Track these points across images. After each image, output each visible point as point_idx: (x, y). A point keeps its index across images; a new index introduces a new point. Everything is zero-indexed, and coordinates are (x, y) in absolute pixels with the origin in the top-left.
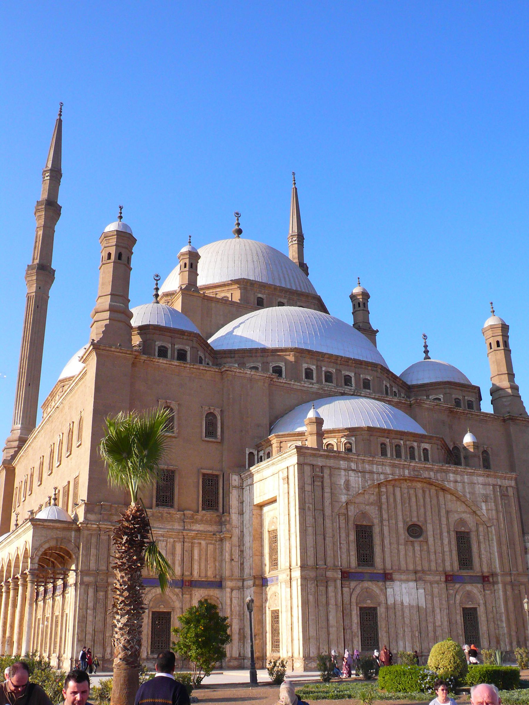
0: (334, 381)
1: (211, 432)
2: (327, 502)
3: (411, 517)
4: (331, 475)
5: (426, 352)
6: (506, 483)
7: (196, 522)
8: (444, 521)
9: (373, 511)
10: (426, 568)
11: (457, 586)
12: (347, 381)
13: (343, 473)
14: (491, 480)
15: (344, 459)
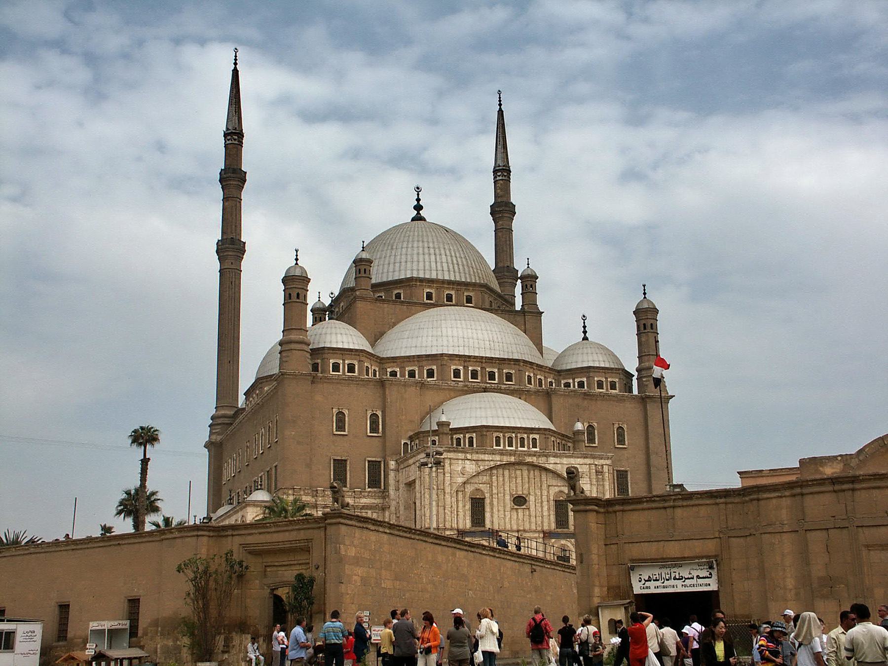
0: (479, 378)
1: (374, 429)
2: (447, 483)
3: (517, 491)
4: (450, 464)
5: (585, 332)
6: (602, 462)
7: (364, 497)
8: (545, 493)
9: (485, 488)
10: (527, 527)
11: (553, 540)
12: (492, 376)
13: (460, 462)
14: (588, 461)
15: (462, 452)
